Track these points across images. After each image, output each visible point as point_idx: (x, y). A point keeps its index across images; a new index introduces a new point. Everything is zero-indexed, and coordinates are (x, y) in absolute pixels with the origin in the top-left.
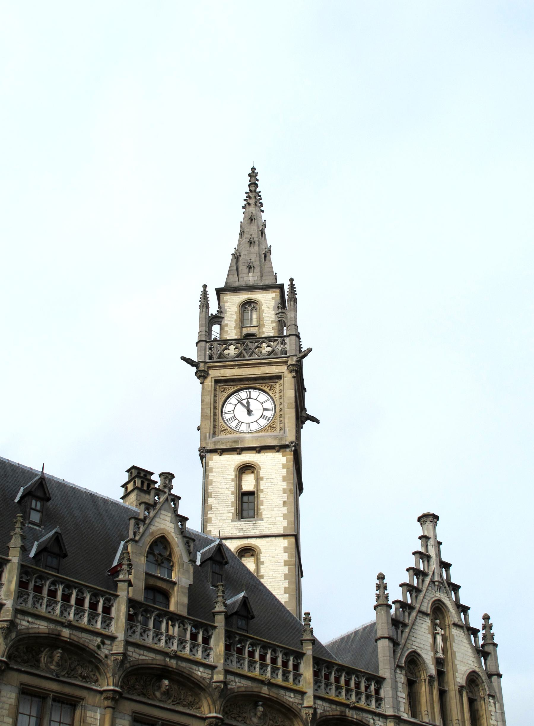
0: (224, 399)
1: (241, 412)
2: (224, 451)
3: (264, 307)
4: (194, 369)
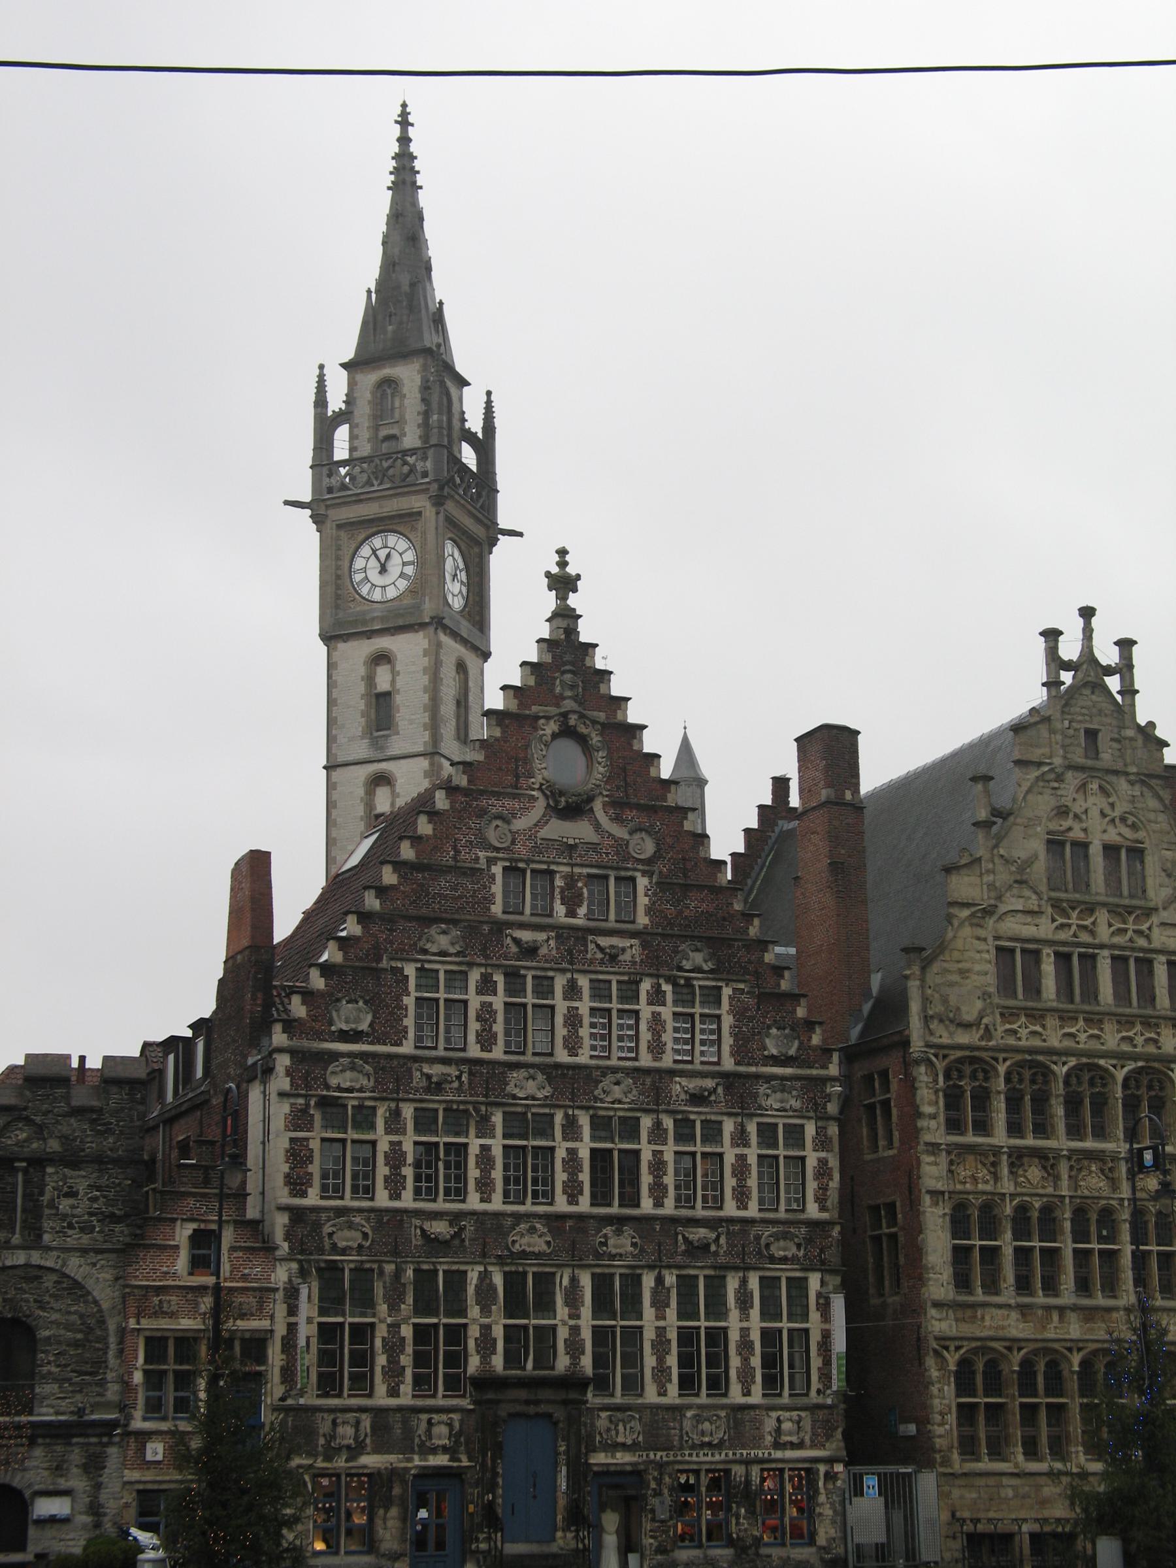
0: (351, 551)
1: (374, 575)
2: (346, 638)
3: (405, 390)
4: (308, 512)
